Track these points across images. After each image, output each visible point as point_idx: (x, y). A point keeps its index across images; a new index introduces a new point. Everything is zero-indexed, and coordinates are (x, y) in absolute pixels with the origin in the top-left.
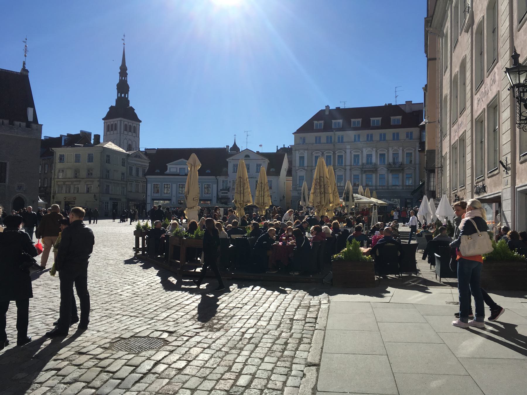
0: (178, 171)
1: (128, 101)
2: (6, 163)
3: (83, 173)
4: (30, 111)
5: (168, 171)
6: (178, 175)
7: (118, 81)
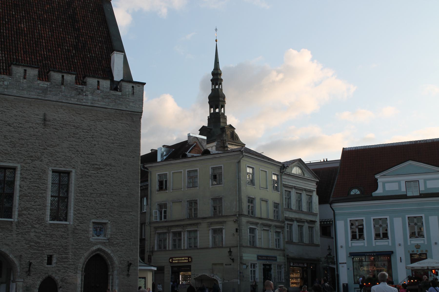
0: (403, 189)
1: (225, 118)
2: (68, 173)
3: (205, 209)
4: (117, 58)
5: (379, 191)
6: (404, 197)
7: (210, 92)
